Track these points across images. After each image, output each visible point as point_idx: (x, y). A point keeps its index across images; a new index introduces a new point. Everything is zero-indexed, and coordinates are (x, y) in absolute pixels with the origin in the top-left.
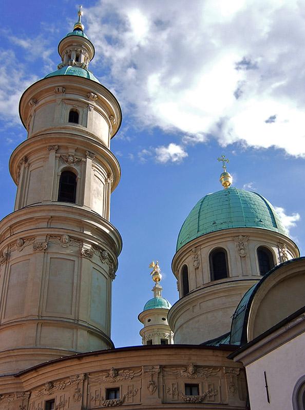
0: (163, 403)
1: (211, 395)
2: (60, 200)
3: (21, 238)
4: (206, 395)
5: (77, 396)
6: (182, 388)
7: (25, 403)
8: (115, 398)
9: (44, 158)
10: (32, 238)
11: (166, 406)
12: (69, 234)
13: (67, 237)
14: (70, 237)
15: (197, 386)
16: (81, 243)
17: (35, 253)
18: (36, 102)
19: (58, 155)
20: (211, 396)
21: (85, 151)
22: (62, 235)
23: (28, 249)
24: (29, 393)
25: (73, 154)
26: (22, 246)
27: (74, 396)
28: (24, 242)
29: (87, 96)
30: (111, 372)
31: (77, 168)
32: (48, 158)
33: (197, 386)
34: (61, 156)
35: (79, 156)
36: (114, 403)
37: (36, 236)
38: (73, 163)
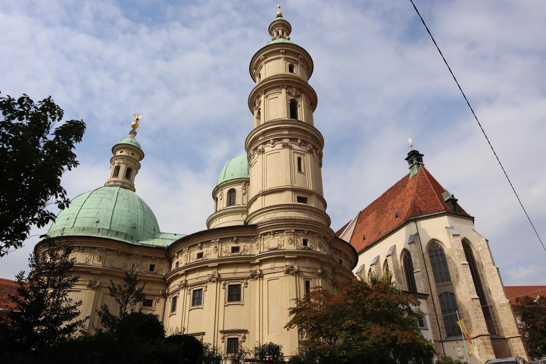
3: (273, 139)
18: (266, 58)
19: (288, 91)
23: (279, 146)
26: (274, 143)
31: (297, 100)
32: (281, 92)
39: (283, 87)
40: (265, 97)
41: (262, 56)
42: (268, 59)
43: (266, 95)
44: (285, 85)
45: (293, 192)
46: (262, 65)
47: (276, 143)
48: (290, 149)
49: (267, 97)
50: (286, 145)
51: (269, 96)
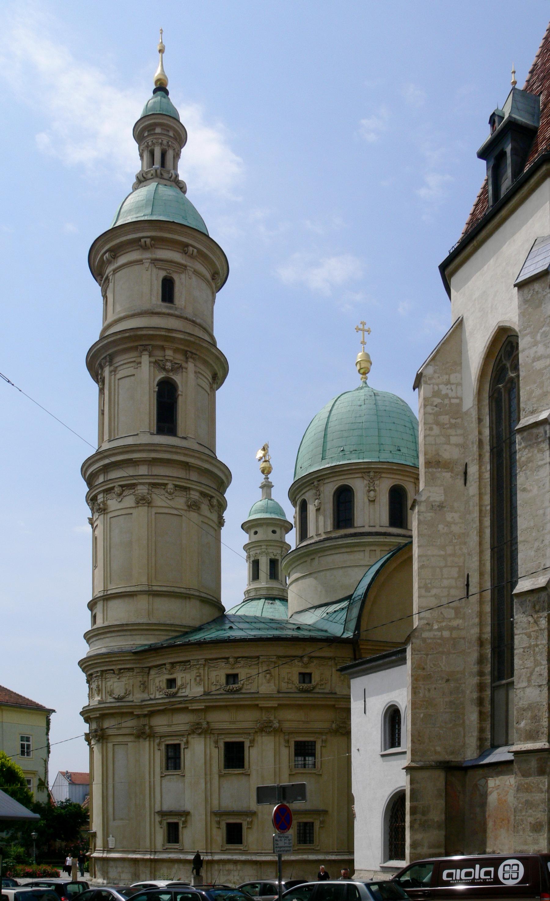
0: (279, 692)
1: (322, 683)
2: (161, 431)
3: (120, 486)
4: (317, 684)
5: (198, 678)
6: (296, 678)
7: (146, 679)
8: (234, 684)
9: (135, 361)
10: (132, 486)
11: (281, 695)
12: (174, 483)
13: (172, 486)
14: (176, 486)
15: (310, 674)
16: (188, 493)
17: (138, 507)
18: (115, 257)
20: (323, 684)
21: (186, 351)
22: (167, 484)
23: (129, 501)
24: (147, 669)
25: (171, 358)
27: (195, 679)
28: (123, 491)
29: (184, 251)
30: (231, 660)
31: (177, 378)
33: (310, 674)
34: (156, 361)
35: (179, 358)
36: (233, 688)
37: (137, 485)
38: (172, 370)
39: (145, 348)
40: (111, 372)
41: (105, 253)
42: (122, 260)
43: (112, 368)
44: (149, 345)
45: (151, 597)
46: (107, 277)
47: (125, 494)
48: (148, 507)
49: (115, 371)
50: (141, 500)
51: (119, 369)
